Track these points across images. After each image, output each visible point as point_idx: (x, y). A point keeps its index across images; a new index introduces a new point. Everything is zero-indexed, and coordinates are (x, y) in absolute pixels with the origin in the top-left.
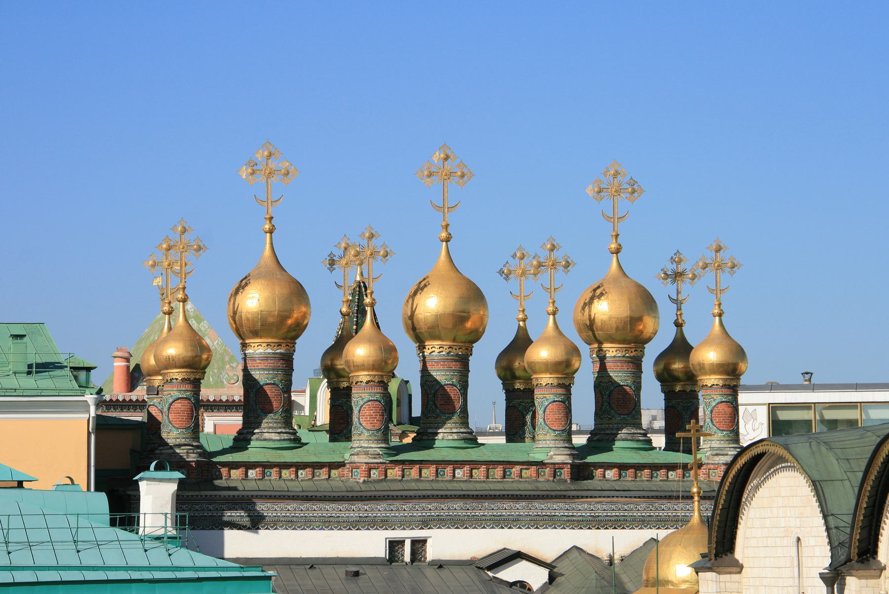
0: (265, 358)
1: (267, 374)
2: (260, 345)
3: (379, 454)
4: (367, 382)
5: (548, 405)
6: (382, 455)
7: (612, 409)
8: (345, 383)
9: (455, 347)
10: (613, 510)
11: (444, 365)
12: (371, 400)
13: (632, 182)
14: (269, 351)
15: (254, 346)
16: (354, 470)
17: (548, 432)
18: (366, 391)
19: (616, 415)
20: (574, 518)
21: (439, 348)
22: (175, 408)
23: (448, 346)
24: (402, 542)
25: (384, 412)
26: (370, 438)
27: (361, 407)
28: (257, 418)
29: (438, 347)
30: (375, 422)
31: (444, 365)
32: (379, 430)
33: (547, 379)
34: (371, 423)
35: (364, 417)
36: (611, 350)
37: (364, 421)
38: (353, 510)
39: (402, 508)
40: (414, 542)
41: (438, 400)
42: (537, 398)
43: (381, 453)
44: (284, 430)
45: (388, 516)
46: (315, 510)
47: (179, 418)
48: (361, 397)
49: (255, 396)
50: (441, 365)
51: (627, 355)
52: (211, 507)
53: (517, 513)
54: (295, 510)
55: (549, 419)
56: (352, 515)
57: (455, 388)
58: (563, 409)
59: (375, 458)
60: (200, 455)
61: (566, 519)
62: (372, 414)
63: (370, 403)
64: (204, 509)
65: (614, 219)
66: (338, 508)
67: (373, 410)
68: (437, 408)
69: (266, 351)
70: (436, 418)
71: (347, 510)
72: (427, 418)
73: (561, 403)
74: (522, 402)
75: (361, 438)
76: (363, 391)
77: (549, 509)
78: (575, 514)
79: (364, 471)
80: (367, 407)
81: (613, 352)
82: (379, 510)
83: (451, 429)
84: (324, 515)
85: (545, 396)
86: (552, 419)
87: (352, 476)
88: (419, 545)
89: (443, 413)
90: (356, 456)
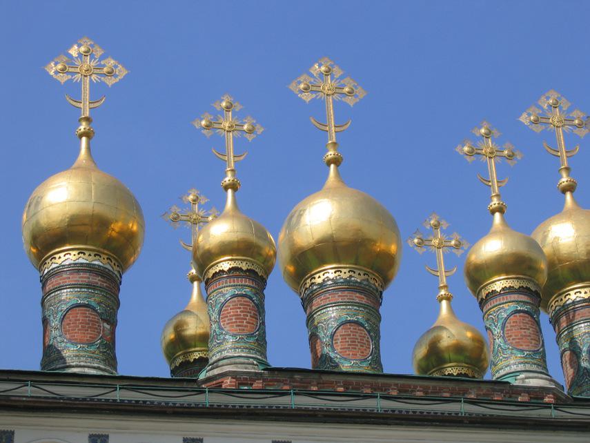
0: (77, 268)
3: (253, 364)
4: (230, 270)
6: (256, 365)
8: (197, 353)
11: (344, 296)
14: (81, 261)
15: (60, 258)
17: (512, 353)
21: (335, 272)
23: (348, 270)
25: (257, 314)
26: (237, 345)
31: (344, 296)
32: (251, 335)
33: (502, 281)
34: (237, 326)
35: (226, 319)
37: (229, 323)
41: (337, 343)
42: (488, 315)
43: (255, 362)
48: (221, 293)
55: (511, 336)
58: (530, 323)
63: (235, 299)
67: (240, 308)
69: (77, 262)
73: (527, 315)
75: (223, 348)
76: (224, 285)
81: (586, 293)
85: (501, 306)
86: (516, 336)
89: (345, 359)
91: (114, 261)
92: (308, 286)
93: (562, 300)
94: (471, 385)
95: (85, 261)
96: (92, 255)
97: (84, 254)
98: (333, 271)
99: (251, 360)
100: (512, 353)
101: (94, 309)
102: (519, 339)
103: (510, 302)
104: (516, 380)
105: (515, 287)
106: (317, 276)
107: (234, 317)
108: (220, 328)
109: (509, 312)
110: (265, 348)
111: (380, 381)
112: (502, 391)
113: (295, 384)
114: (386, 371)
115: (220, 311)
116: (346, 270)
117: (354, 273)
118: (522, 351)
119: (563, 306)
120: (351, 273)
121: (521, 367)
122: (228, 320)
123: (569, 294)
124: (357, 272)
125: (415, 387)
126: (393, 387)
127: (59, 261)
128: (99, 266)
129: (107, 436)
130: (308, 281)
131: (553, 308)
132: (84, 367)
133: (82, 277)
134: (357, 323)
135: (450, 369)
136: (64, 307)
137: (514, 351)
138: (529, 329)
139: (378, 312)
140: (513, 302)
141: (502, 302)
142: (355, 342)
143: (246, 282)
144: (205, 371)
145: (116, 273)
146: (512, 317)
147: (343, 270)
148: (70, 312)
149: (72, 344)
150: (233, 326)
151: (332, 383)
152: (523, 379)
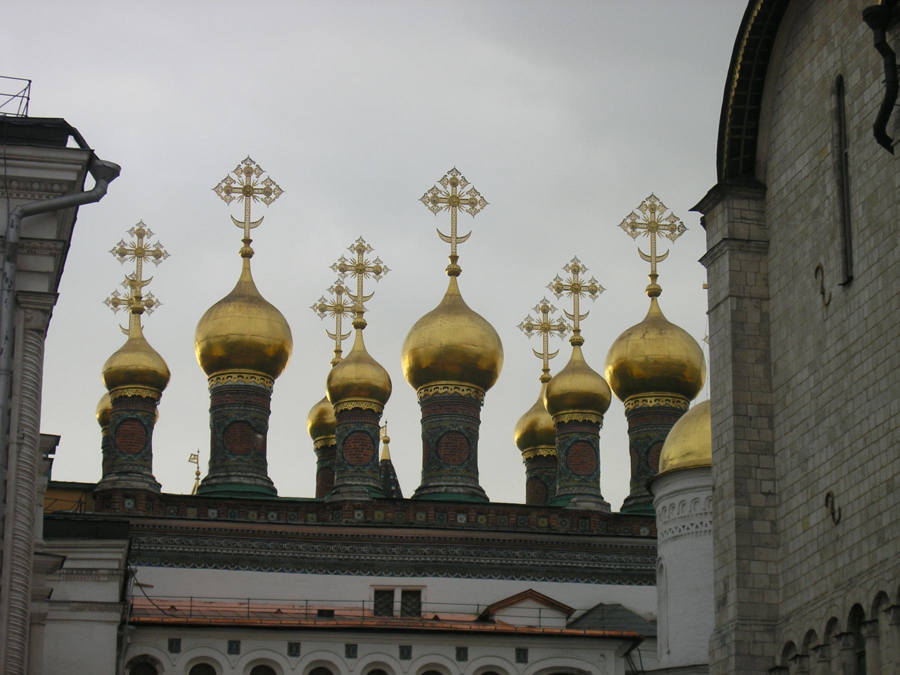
1: (237, 410)
2: (229, 377)
3: (365, 492)
5: (572, 445)
7: (650, 468)
9: (462, 388)
10: (649, 563)
16: (335, 512)
18: (351, 420)
20: (601, 571)
22: (123, 431)
23: (454, 386)
24: (391, 593)
28: (224, 460)
30: (362, 456)
35: (348, 451)
36: (649, 399)
38: (331, 551)
39: (391, 550)
40: (406, 593)
43: (367, 491)
44: (255, 475)
45: (374, 560)
46: (284, 549)
47: (127, 442)
49: (223, 434)
50: (445, 409)
51: (667, 406)
52: (159, 540)
53: (531, 563)
54: (261, 547)
56: (329, 556)
57: (461, 436)
59: (360, 497)
60: (151, 484)
61: (590, 571)
62: (358, 446)
63: (355, 434)
64: (150, 542)
65: (653, 259)
66: (313, 548)
67: (358, 442)
68: (440, 458)
69: (237, 383)
70: (439, 470)
71: (324, 550)
72: (429, 472)
73: (587, 444)
74: (545, 472)
77: (570, 558)
78: (602, 566)
79: (347, 511)
81: (651, 402)
82: (363, 552)
83: (456, 482)
84: (297, 555)
87: (332, 519)
88: (413, 596)
90: (337, 495)
95: (243, 384)
96: (249, 378)
97: (243, 377)
98: (442, 387)
99: (364, 488)
100: (570, 477)
101: (250, 425)
103: (574, 433)
104: (570, 502)
105: (579, 420)
106: (430, 389)
107: (354, 450)
109: (573, 441)
111: (462, 506)
115: (344, 443)
116: (453, 387)
118: (579, 475)
119: (634, 409)
120: (457, 390)
121: (576, 491)
122: (350, 452)
123: (638, 401)
126: (472, 511)
128: (255, 387)
129: (239, 642)
130: (423, 391)
132: (241, 476)
133: (241, 398)
134: (459, 432)
135: (541, 450)
136: (227, 423)
137: (573, 476)
138: (586, 456)
140: (576, 433)
141: (568, 431)
142: (455, 449)
143: (364, 419)
144: (330, 495)
145: (268, 389)
146: (574, 446)
147: (450, 387)
152: (575, 504)
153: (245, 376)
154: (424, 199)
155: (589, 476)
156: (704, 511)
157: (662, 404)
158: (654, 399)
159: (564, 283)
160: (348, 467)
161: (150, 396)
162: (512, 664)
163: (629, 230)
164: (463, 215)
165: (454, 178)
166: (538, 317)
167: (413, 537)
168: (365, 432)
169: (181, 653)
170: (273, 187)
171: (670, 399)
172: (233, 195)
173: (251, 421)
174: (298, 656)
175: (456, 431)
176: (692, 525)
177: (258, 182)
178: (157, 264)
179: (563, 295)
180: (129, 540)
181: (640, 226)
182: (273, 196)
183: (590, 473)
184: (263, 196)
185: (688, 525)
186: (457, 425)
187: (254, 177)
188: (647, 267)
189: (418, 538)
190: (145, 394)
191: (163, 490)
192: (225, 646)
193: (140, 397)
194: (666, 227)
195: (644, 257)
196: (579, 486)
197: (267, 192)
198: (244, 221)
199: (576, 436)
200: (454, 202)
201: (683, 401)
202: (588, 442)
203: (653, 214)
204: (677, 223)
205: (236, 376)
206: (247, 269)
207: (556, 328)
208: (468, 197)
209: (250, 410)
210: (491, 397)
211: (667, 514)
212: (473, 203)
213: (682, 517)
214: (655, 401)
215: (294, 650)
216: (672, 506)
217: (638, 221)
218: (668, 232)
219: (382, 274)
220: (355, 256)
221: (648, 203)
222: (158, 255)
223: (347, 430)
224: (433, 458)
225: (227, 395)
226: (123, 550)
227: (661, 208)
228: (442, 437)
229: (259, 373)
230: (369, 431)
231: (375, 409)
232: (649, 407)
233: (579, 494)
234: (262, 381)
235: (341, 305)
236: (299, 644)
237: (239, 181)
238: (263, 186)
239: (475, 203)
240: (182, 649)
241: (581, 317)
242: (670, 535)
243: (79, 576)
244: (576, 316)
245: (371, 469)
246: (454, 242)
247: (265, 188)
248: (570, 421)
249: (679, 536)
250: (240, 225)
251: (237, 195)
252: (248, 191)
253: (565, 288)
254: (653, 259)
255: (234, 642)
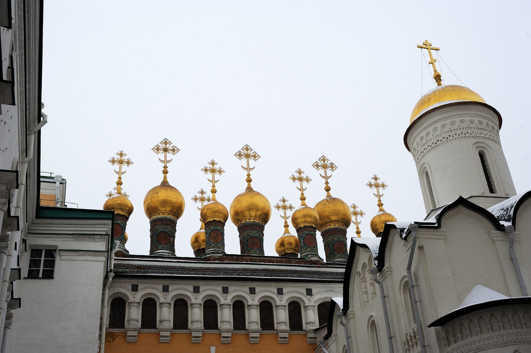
12: (215, 229)
13: (332, 164)
19: (337, 254)
27: (210, 233)
28: (157, 247)
29: (248, 219)
36: (332, 225)
43: (220, 252)
49: (156, 237)
63: (214, 231)
65: (326, 177)
68: (249, 247)
70: (249, 252)
80: (213, 232)
81: (332, 226)
91: (174, 217)
92: (239, 224)
93: (325, 228)
94: (292, 260)
97: (164, 214)
98: (248, 219)
102: (309, 243)
106: (242, 221)
108: (209, 240)
110: (224, 247)
111: (262, 258)
112: (302, 261)
113: (234, 260)
114: (265, 255)
115: (209, 235)
116: (252, 219)
117: (255, 220)
118: (309, 247)
120: (254, 220)
121: (309, 253)
124: (256, 220)
125: (274, 260)
127: (156, 217)
128: (169, 218)
129: (169, 286)
131: (322, 231)
134: (256, 237)
139: (263, 233)
143: (218, 225)
147: (251, 219)
148: (159, 234)
149: (160, 245)
150: (213, 240)
151: (246, 259)
152: (309, 258)
153: (165, 214)
154: (235, 155)
155: (314, 248)
156: (450, 129)
157: (337, 227)
158: (334, 225)
159: (296, 177)
160: (212, 244)
161: (124, 214)
162: (305, 296)
163: (316, 167)
164: (251, 161)
165: (247, 148)
166: (281, 204)
167: (242, 269)
168: (219, 230)
169: (138, 291)
170: (176, 149)
171: (340, 225)
172: (159, 151)
173: (168, 232)
174: (199, 293)
175: (255, 237)
176: (443, 138)
177: (170, 147)
178: (128, 166)
179: (296, 181)
180: (111, 220)
181: (320, 166)
182: (176, 152)
183: (314, 247)
184: (172, 152)
185: (440, 138)
186: (255, 234)
187: (168, 145)
188: (324, 181)
189: (244, 269)
190: (122, 213)
191: (129, 254)
192: (161, 288)
193: (120, 214)
194: (330, 167)
195: (322, 177)
196: (310, 252)
197: (173, 150)
198: (164, 160)
199: (307, 232)
200: (248, 156)
201: (345, 227)
202: (312, 234)
203: (324, 162)
204: (334, 165)
205: (162, 214)
206: (165, 178)
207: (288, 207)
208: (253, 154)
209: (168, 228)
210: (267, 227)
211: (425, 139)
212: (255, 156)
213: (436, 136)
214: (334, 226)
215: (196, 290)
216: (428, 134)
217: (319, 164)
218: (331, 169)
219: (222, 173)
220: (211, 166)
221: (322, 158)
222: (128, 163)
223: (210, 229)
224: (246, 247)
225: (158, 222)
226: (108, 226)
227: (327, 160)
228: (249, 239)
229: (171, 213)
230: (220, 230)
231: (222, 221)
232: (332, 228)
233: (311, 255)
234: (173, 216)
235: (203, 198)
236: (199, 287)
237: (162, 146)
238: (172, 148)
239: (255, 157)
240: (139, 289)
241: (304, 190)
242: (429, 148)
243: (84, 239)
244: (302, 189)
245: (221, 244)
246: (248, 170)
247: (173, 149)
248: (304, 226)
249: (435, 146)
250: (163, 162)
251: (161, 151)
252: (166, 150)
253: (296, 179)
254: (326, 177)
255: (166, 286)
